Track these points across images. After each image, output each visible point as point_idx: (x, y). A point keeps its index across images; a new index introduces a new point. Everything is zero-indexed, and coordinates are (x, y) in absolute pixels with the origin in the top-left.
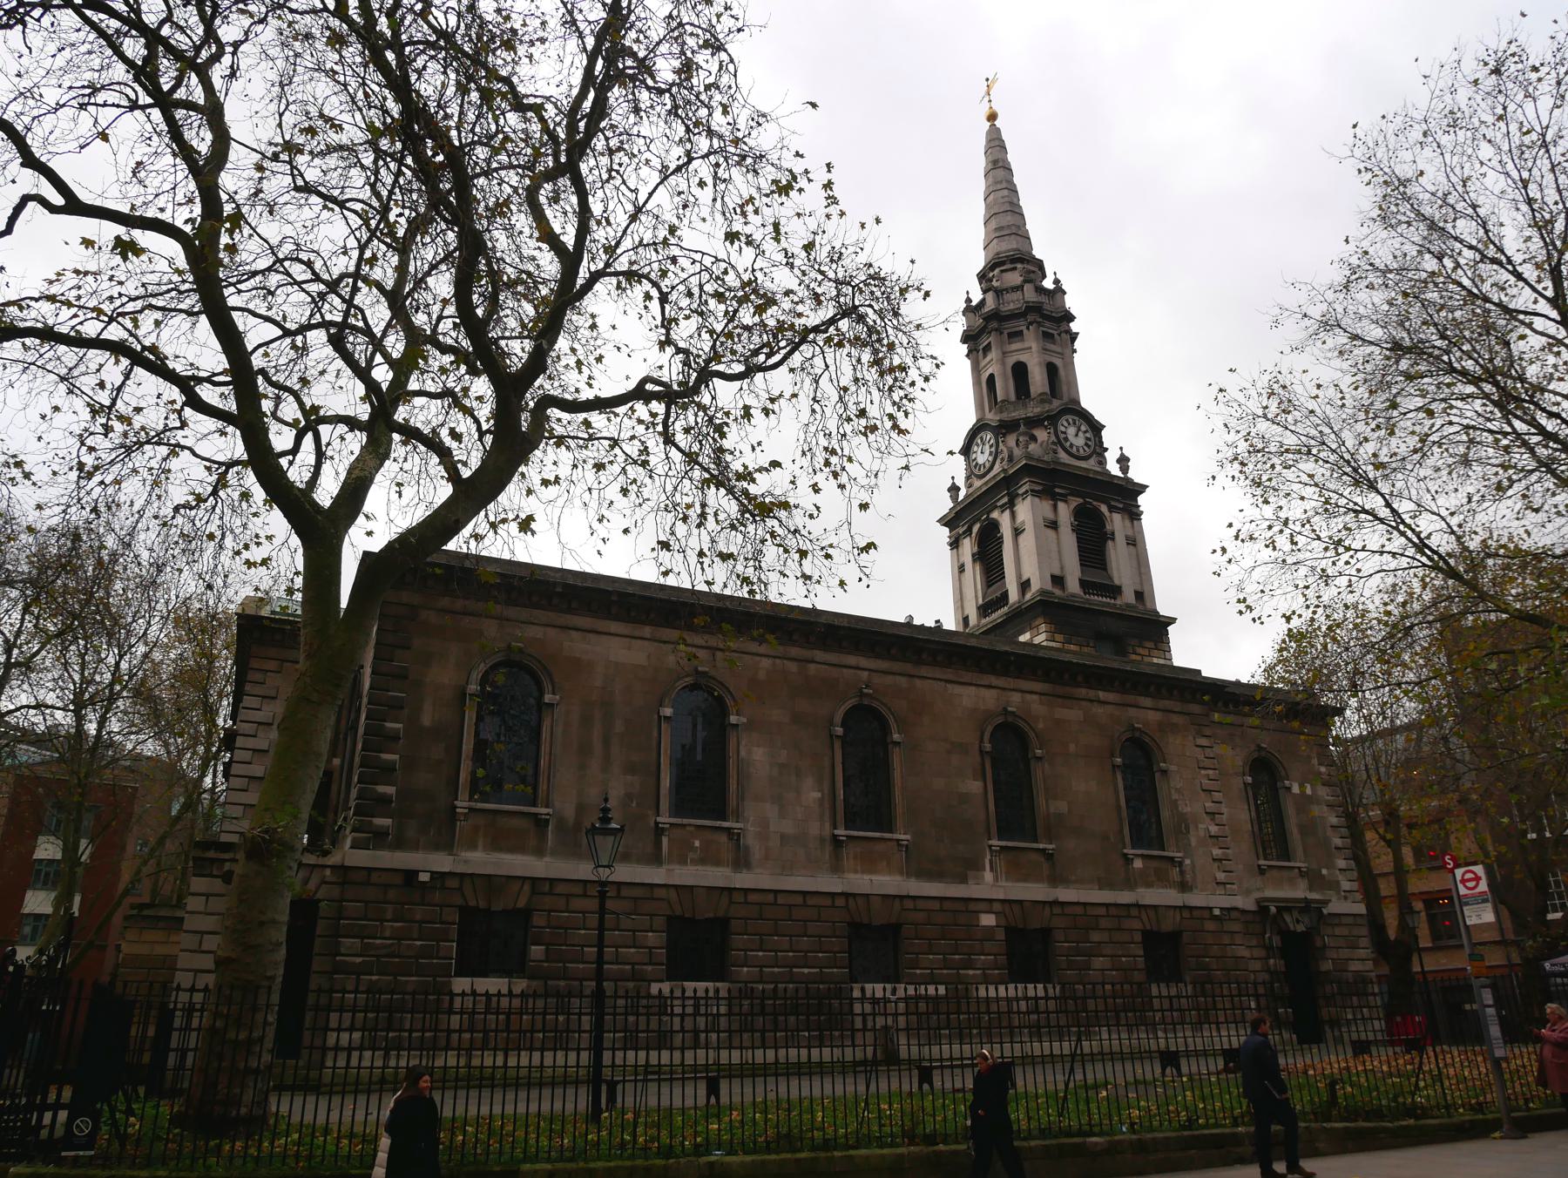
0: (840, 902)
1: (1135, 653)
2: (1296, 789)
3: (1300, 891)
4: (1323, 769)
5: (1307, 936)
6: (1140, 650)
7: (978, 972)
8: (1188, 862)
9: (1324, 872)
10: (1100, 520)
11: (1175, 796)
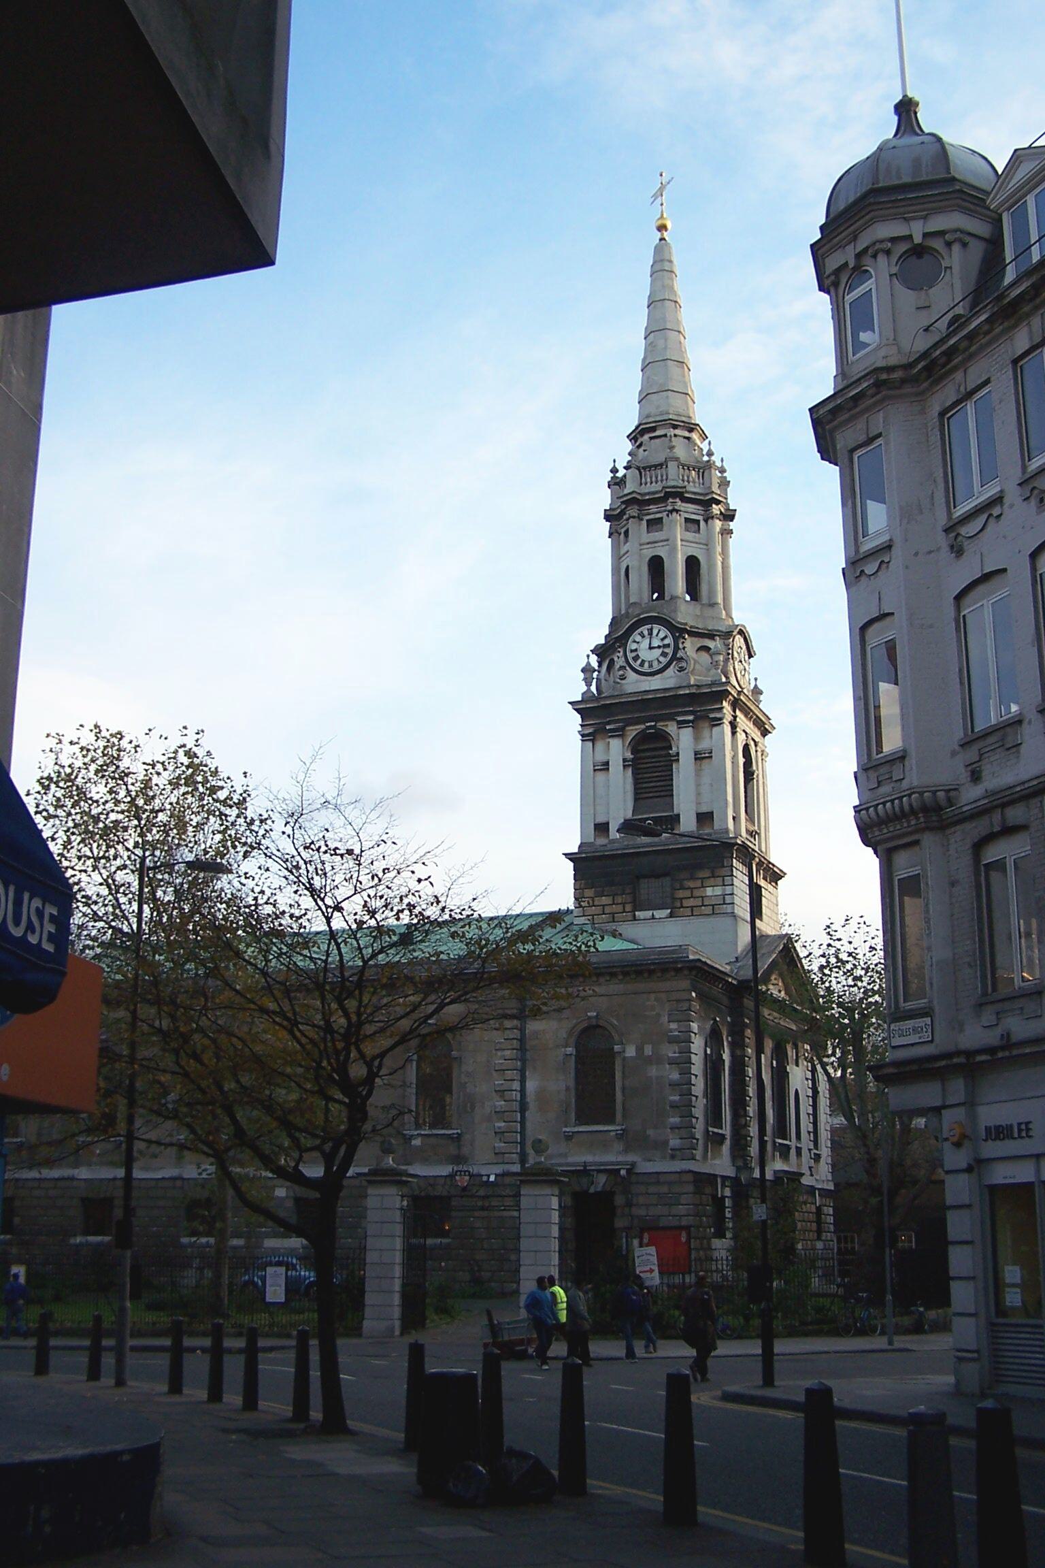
0: (179, 1183)
1: (682, 888)
2: (631, 1052)
3: (612, 1156)
4: (673, 1026)
5: (606, 1197)
6: (691, 884)
7: (270, 1230)
8: (467, 1137)
9: (650, 1132)
10: (664, 740)
11: (464, 1079)
